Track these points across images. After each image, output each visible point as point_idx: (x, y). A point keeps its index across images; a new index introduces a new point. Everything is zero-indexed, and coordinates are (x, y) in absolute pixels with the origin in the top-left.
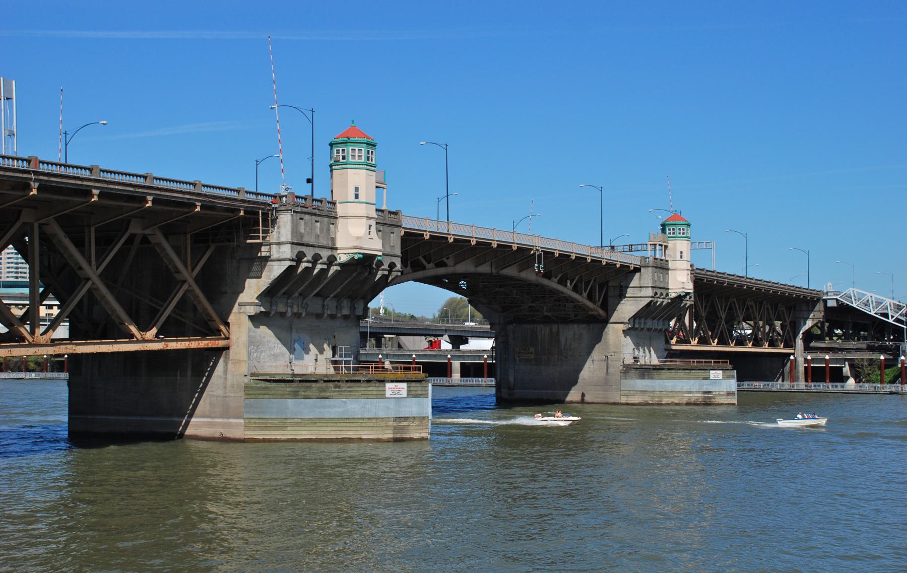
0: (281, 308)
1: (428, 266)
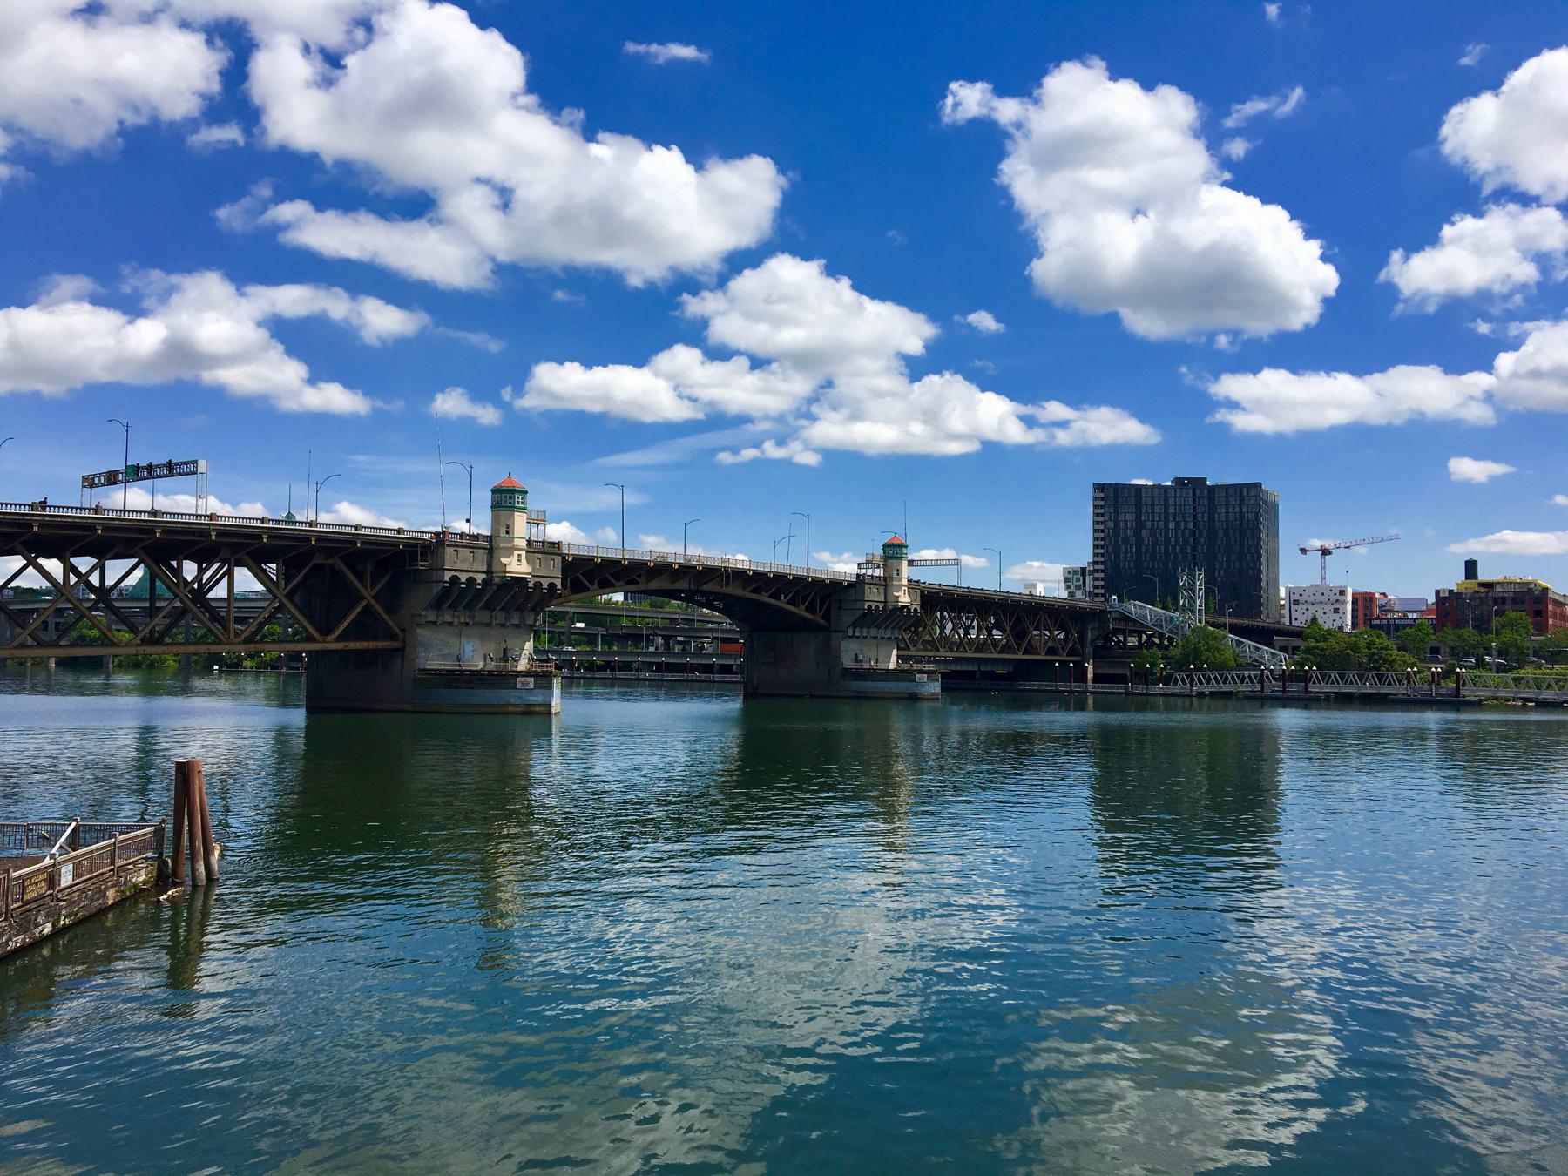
0: (448, 618)
1: (591, 587)
